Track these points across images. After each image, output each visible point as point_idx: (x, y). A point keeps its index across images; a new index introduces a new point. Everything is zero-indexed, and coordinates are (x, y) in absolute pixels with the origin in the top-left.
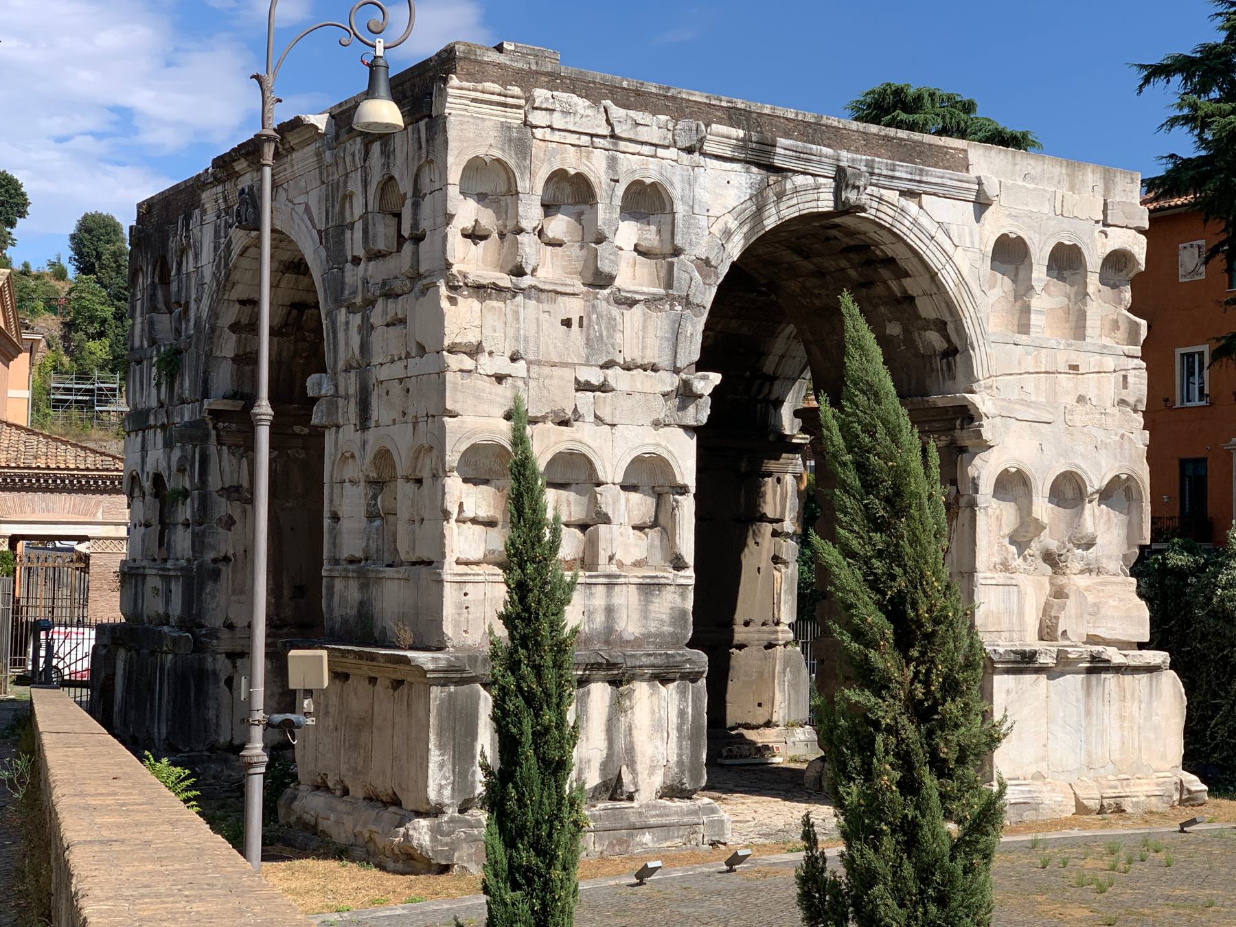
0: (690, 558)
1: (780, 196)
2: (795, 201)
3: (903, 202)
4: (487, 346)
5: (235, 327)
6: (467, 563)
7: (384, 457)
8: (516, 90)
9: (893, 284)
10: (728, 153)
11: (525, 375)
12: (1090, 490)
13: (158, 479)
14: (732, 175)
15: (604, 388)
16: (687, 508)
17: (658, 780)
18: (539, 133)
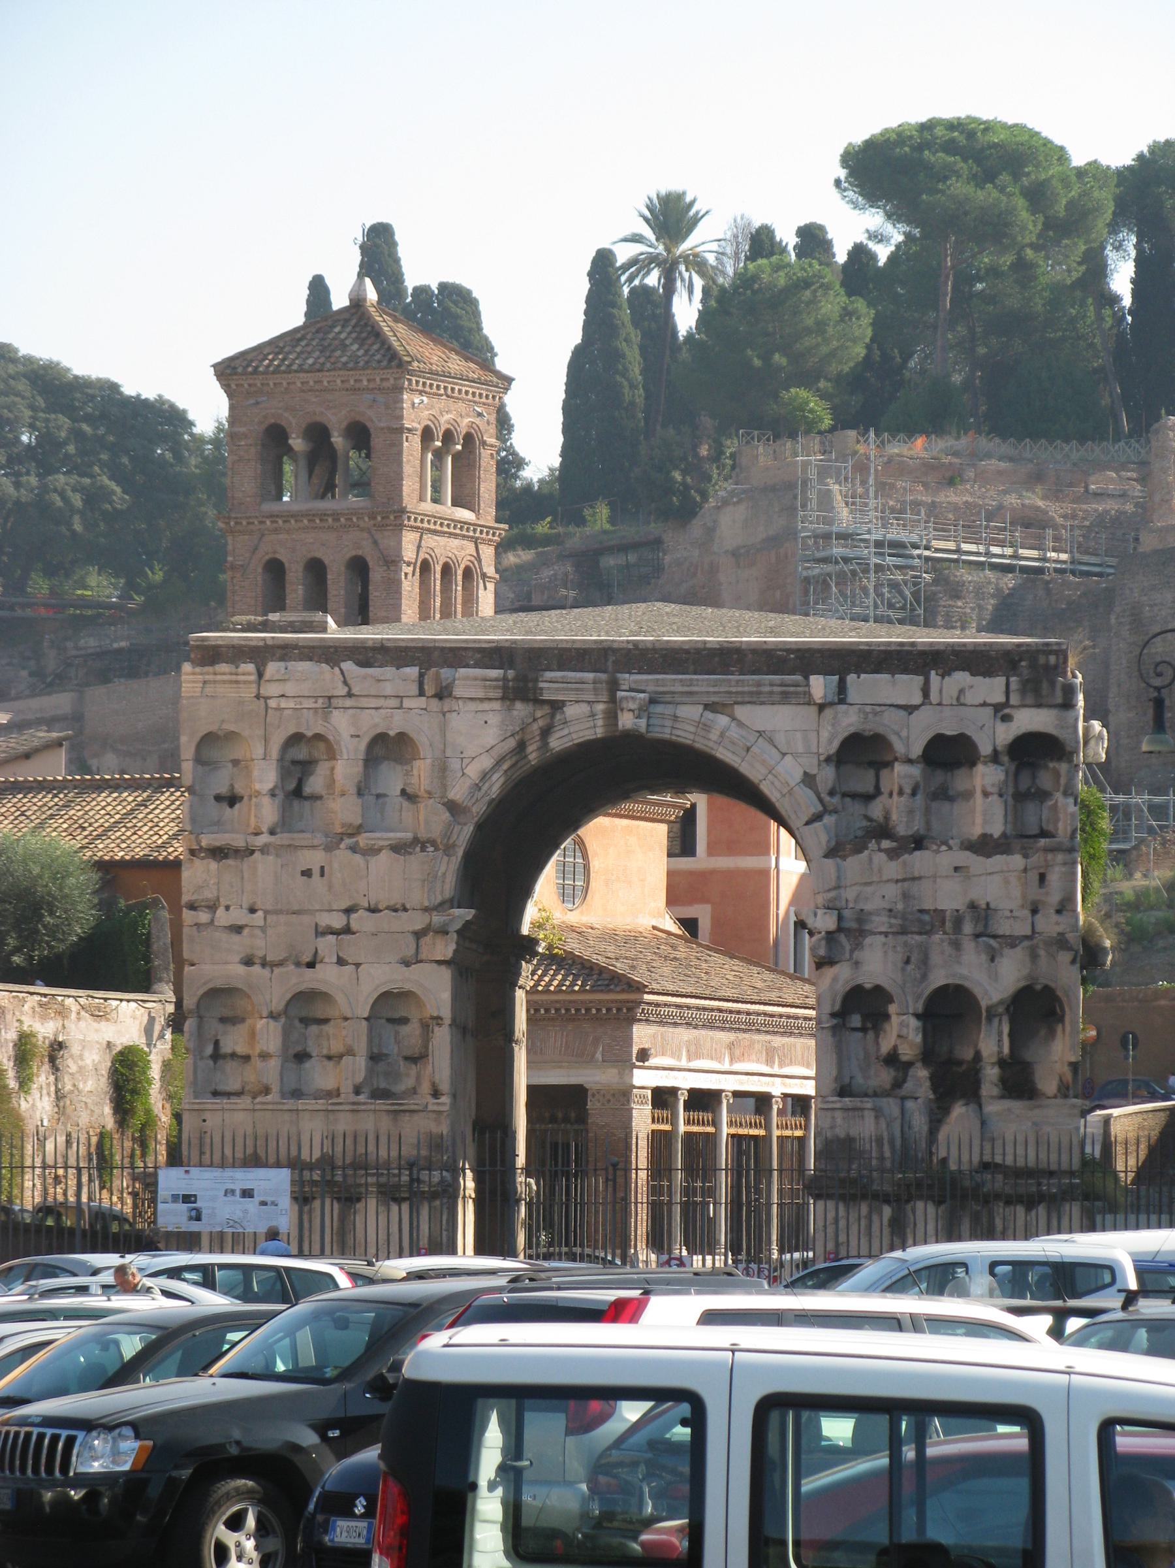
0: (445, 1086)
1: (546, 732)
2: (566, 732)
3: (709, 715)
4: (223, 902)
6: (228, 1094)
8: (250, 667)
10: (481, 695)
11: (261, 923)
12: (984, 1004)
14: (491, 714)
15: (347, 930)
18: (272, 703)
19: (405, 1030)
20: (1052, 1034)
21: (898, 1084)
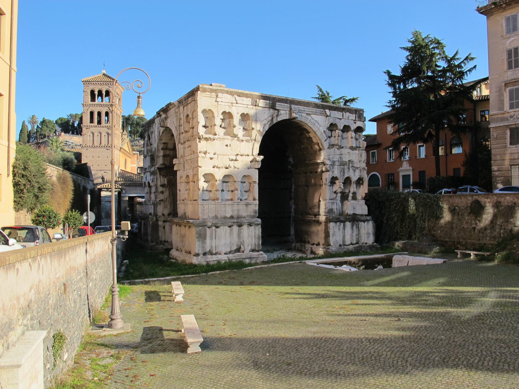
0: (257, 198)
1: (277, 116)
5: (162, 149)
6: (205, 200)
7: (188, 176)
8: (214, 94)
9: (307, 135)
13: (149, 183)
15: (236, 160)
16: (257, 186)
17: (250, 248)
19: (245, 184)
20: (360, 187)
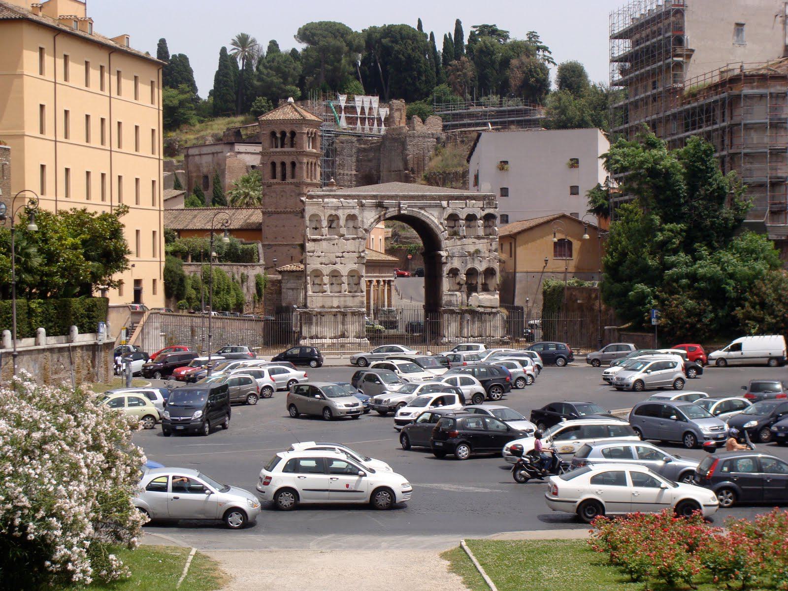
1: (385, 214)
15: (343, 257)
20: (492, 278)
21: (460, 289)
